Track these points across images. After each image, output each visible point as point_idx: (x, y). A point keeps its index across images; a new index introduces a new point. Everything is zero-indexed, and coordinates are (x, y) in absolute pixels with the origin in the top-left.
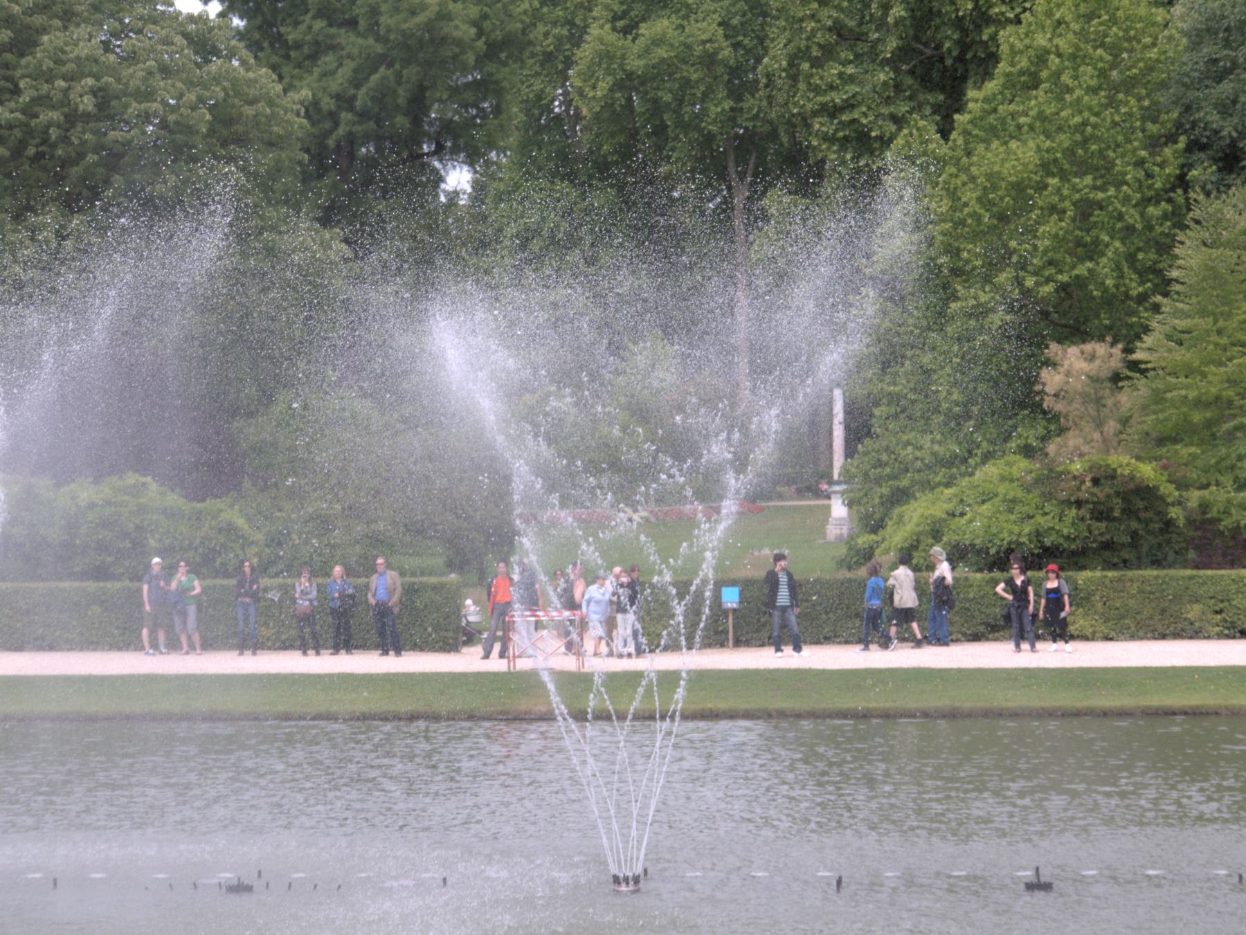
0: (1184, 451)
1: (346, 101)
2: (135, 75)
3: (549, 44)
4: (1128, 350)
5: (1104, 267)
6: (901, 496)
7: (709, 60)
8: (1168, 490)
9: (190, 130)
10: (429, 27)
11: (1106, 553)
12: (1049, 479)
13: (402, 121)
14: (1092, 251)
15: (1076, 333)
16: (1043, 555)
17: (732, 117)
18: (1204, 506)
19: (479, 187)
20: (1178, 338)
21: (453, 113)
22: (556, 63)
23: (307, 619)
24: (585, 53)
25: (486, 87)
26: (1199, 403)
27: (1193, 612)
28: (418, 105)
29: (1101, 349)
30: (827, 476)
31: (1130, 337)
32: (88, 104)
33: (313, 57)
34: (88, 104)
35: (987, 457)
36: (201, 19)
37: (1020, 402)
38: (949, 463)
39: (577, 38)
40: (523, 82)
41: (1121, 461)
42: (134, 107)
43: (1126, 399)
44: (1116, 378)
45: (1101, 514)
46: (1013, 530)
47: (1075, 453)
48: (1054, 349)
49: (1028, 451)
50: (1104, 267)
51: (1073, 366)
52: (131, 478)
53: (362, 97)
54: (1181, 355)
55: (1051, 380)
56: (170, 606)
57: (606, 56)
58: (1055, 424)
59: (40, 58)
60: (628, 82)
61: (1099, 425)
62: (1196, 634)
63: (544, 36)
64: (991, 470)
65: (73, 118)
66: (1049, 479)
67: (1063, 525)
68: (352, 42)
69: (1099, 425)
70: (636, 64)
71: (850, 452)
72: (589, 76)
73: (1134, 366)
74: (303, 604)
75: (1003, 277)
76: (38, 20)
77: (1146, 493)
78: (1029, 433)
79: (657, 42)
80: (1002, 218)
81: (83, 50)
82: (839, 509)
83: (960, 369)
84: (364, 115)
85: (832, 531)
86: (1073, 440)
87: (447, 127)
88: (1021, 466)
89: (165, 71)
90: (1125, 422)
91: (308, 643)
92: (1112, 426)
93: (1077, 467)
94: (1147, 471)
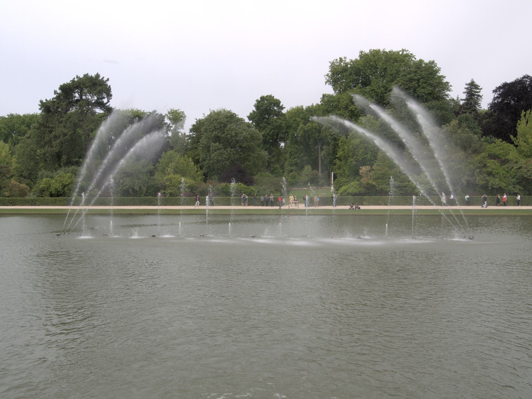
0: (379, 180)
1: (268, 134)
2: (240, 130)
3: (294, 127)
4: (372, 167)
5: (369, 156)
6: (340, 186)
7: (316, 129)
8: (377, 185)
9: (247, 138)
10: (280, 125)
11: (368, 194)
12: (361, 184)
13: (275, 137)
14: (367, 154)
15: (364, 164)
16: (360, 194)
17: (319, 136)
18: (382, 188)
19: (285, 145)
20: (378, 165)
21: (282, 135)
22: (295, 129)
23: (262, 202)
24: (299, 128)
25: (287, 132)
26: (381, 174)
27: (380, 202)
28: (278, 134)
29: (367, 167)
30: (331, 184)
31: (372, 165)
32: (234, 134)
33: (264, 129)
34: (234, 134)
35: (352, 181)
36: (248, 123)
37: (356, 173)
38: (347, 182)
39: (298, 125)
40: (291, 131)
41: (370, 182)
42: (240, 135)
43: (371, 174)
44: (370, 171)
45: (368, 189)
46: (355, 191)
47: (364, 181)
48: (361, 167)
49: (358, 180)
50: (369, 156)
51: (364, 169)
52: (240, 183)
53: (271, 133)
54: (379, 168)
55: (361, 171)
56: (245, 200)
57: (302, 128)
58: (361, 177)
59: (228, 128)
60: (305, 132)
61: (367, 177)
62: (380, 205)
63: (294, 126)
64: (353, 183)
65: (232, 136)
66: (361, 184)
67: (363, 190)
68: (270, 127)
69: (367, 177)
70: (306, 129)
71: (334, 180)
72: (300, 131)
73: (373, 169)
74: (262, 200)
75: (355, 157)
76: (227, 123)
77: (374, 186)
78: (358, 178)
79: (309, 126)
80: (355, 149)
81: (233, 127)
82: (332, 188)
83: (349, 169)
84: (270, 136)
85: (331, 191)
86: (364, 179)
87: (281, 138)
88: (357, 182)
89: (244, 130)
90: (371, 176)
91: (263, 205)
92: (369, 177)
93: (364, 183)
94: (374, 183)
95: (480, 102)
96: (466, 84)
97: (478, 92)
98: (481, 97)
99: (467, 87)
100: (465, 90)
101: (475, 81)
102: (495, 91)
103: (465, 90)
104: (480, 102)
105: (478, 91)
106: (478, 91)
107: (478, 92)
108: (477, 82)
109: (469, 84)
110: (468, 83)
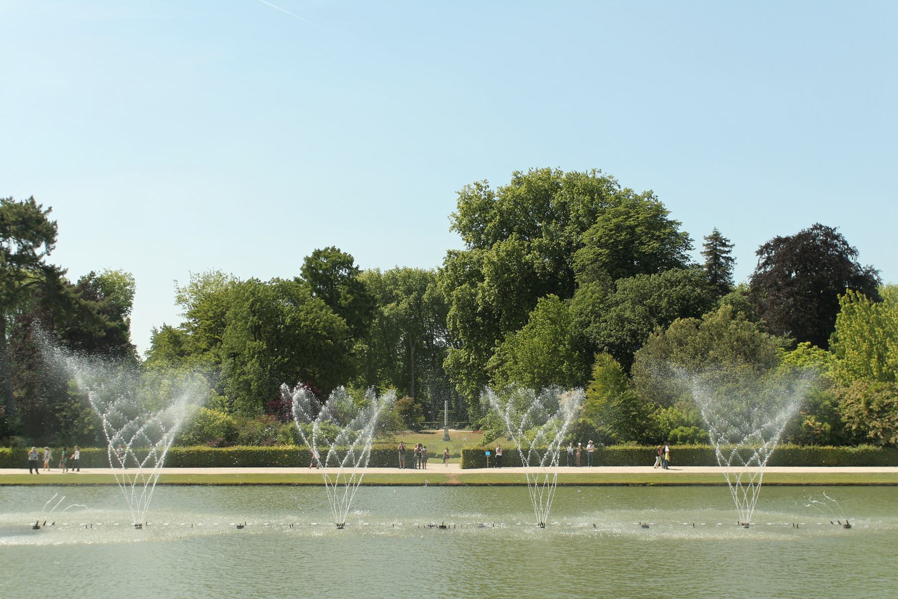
95: (731, 271)
96: (706, 238)
97: (729, 251)
98: (732, 260)
99: (706, 242)
100: (704, 249)
101: (720, 231)
102: (760, 253)
103: (704, 249)
104: (731, 271)
105: (726, 249)
106: (726, 249)
107: (729, 251)
108: (724, 235)
109: (711, 238)
110: (707, 236)
